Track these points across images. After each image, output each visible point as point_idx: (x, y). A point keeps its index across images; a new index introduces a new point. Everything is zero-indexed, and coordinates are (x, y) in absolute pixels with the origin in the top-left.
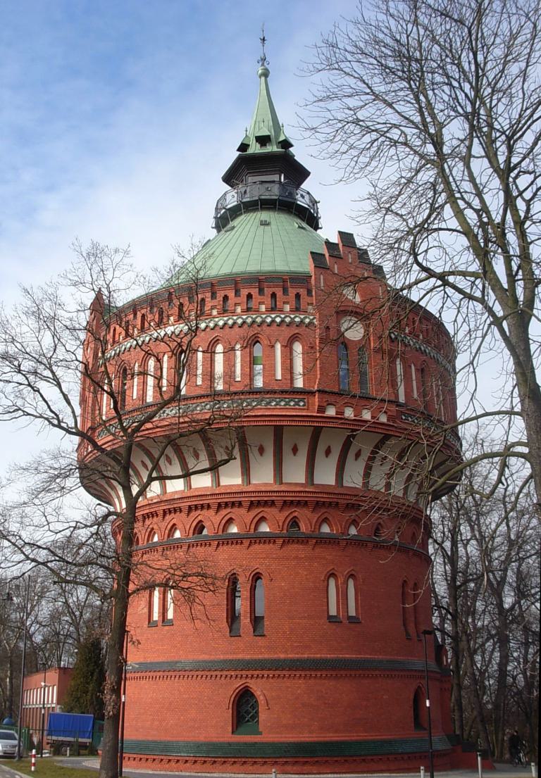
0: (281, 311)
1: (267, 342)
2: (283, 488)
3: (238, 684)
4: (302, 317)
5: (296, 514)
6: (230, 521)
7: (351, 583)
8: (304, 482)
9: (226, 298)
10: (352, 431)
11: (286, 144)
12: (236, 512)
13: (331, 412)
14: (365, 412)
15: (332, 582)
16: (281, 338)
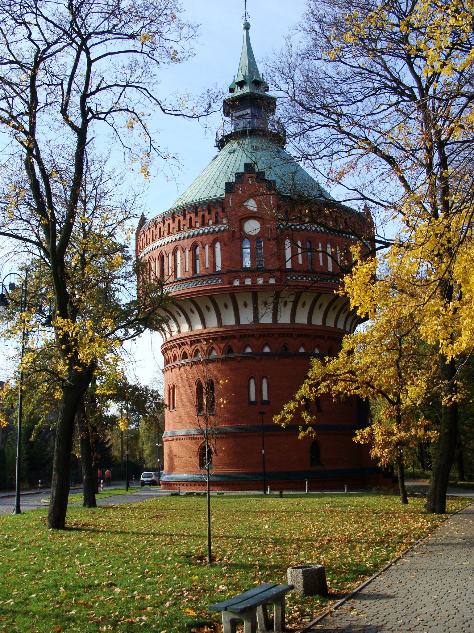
1: (201, 246)
2: (221, 329)
5: (230, 344)
6: (197, 351)
7: (265, 382)
8: (234, 324)
9: (179, 221)
10: (254, 292)
11: (258, 83)
12: (198, 346)
13: (237, 283)
14: (259, 279)
15: (252, 383)
16: (208, 243)
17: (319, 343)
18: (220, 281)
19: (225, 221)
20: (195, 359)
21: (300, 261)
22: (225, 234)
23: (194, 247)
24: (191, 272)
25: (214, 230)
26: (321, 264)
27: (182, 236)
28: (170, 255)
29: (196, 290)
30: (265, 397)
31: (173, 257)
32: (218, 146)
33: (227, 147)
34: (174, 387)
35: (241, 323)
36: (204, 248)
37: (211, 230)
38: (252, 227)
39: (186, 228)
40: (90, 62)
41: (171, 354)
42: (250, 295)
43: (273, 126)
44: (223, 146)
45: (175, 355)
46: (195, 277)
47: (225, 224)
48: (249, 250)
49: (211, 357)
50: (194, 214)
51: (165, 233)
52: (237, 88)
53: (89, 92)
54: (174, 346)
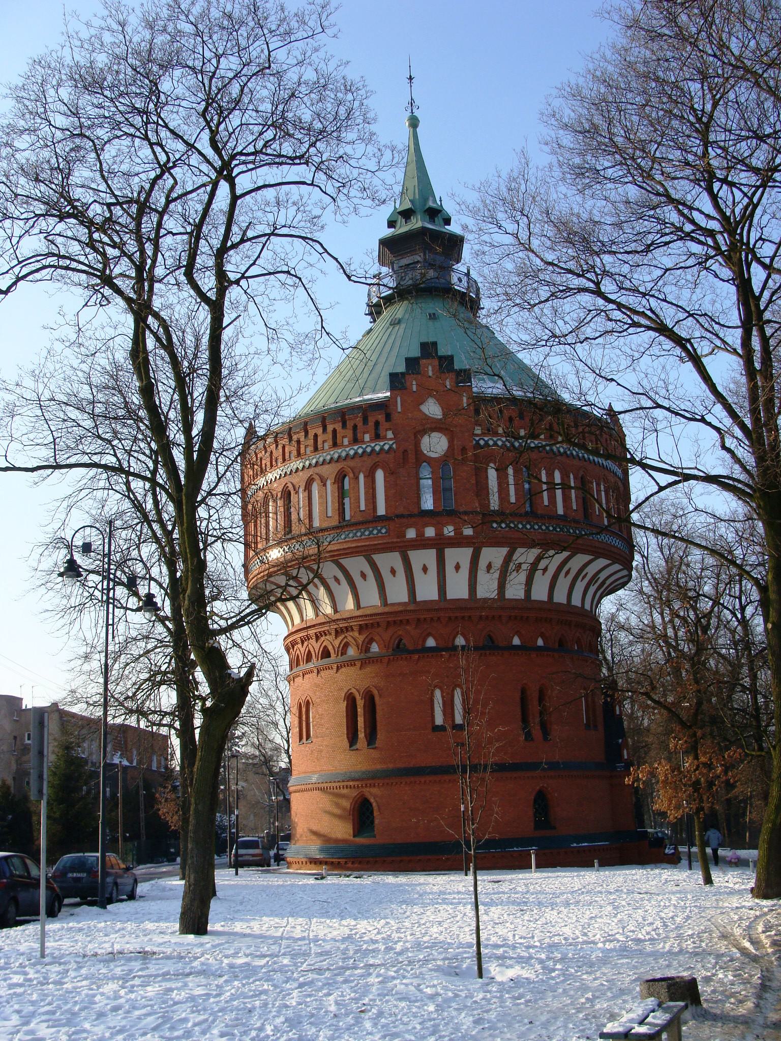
0: (363, 442)
1: (351, 475)
2: (387, 609)
3: (354, 793)
4: (382, 444)
5: (400, 633)
6: (346, 645)
9: (316, 436)
11: (435, 213)
13: (411, 534)
15: (438, 693)
16: (364, 469)
17: (543, 630)
18: (384, 531)
19: (390, 434)
20: (344, 658)
21: (513, 499)
22: (392, 455)
23: (340, 478)
24: (337, 517)
25: (373, 450)
26: (546, 503)
27: (321, 459)
28: (301, 490)
29: (345, 546)
30: (459, 720)
31: (306, 494)
32: (371, 314)
33: (386, 314)
34: (308, 703)
35: (418, 599)
36: (357, 478)
37: (369, 450)
38: (435, 445)
39: (326, 446)
40: (235, 198)
41: (302, 650)
42: (432, 553)
43: (460, 280)
44: (379, 313)
45: (309, 651)
46: (343, 525)
47: (391, 439)
48: (430, 482)
49: (369, 655)
50: (340, 424)
51: (292, 455)
52: (400, 220)
53: (229, 244)
54: (308, 638)
